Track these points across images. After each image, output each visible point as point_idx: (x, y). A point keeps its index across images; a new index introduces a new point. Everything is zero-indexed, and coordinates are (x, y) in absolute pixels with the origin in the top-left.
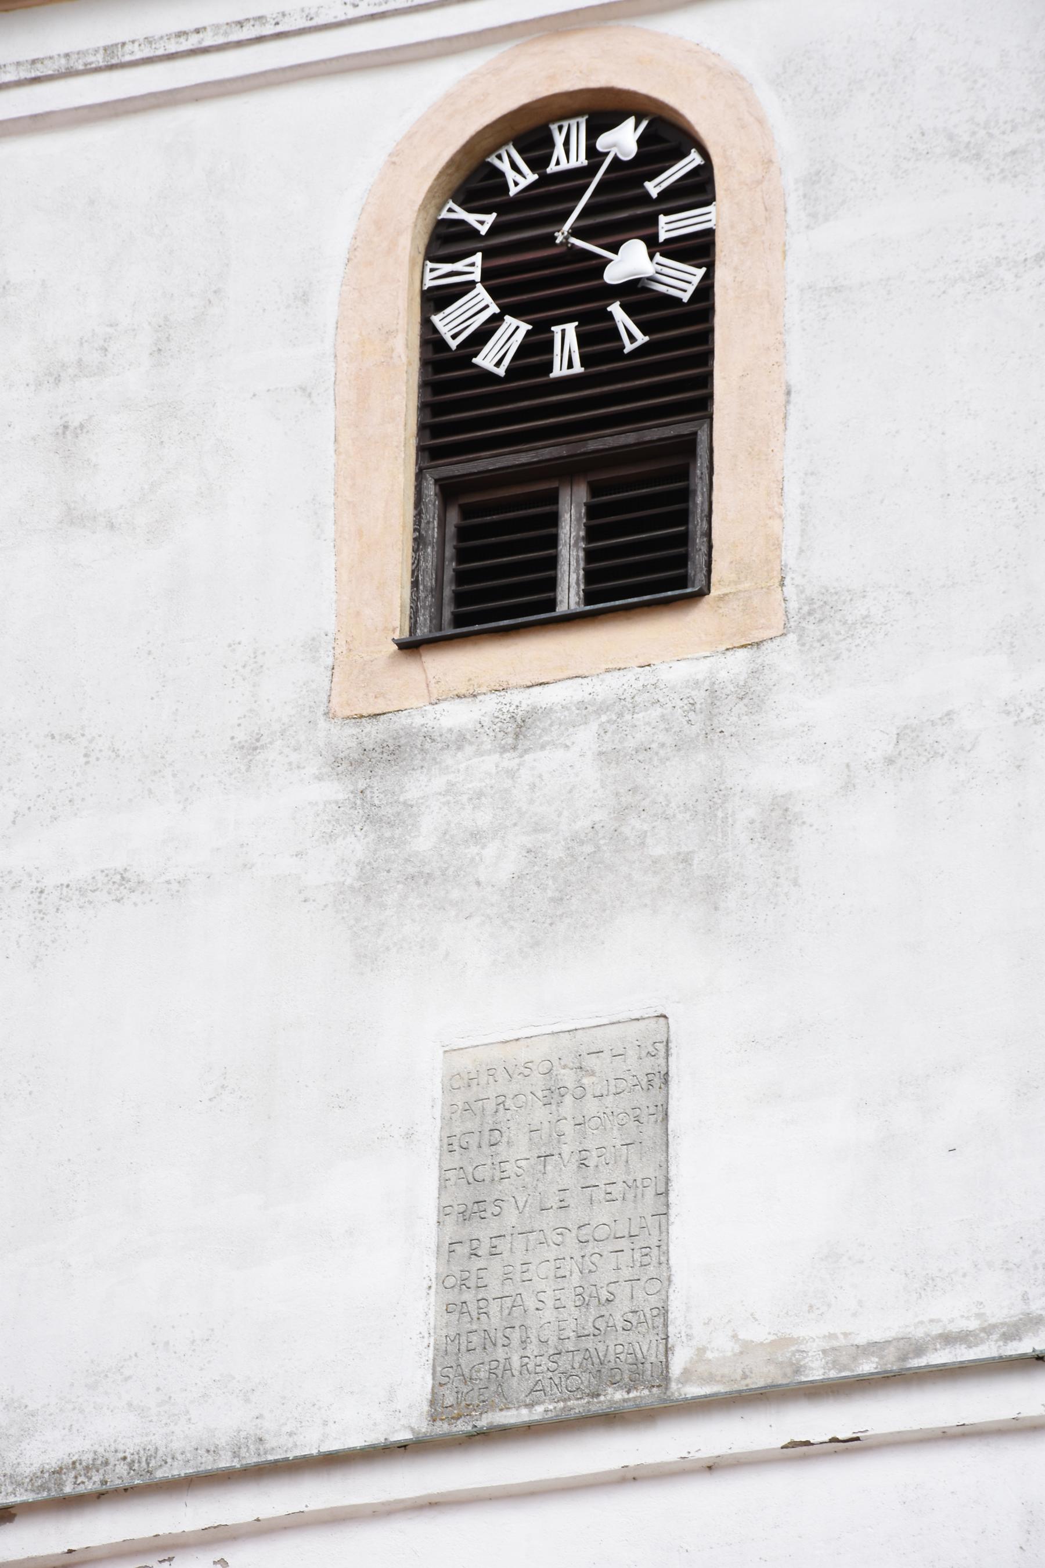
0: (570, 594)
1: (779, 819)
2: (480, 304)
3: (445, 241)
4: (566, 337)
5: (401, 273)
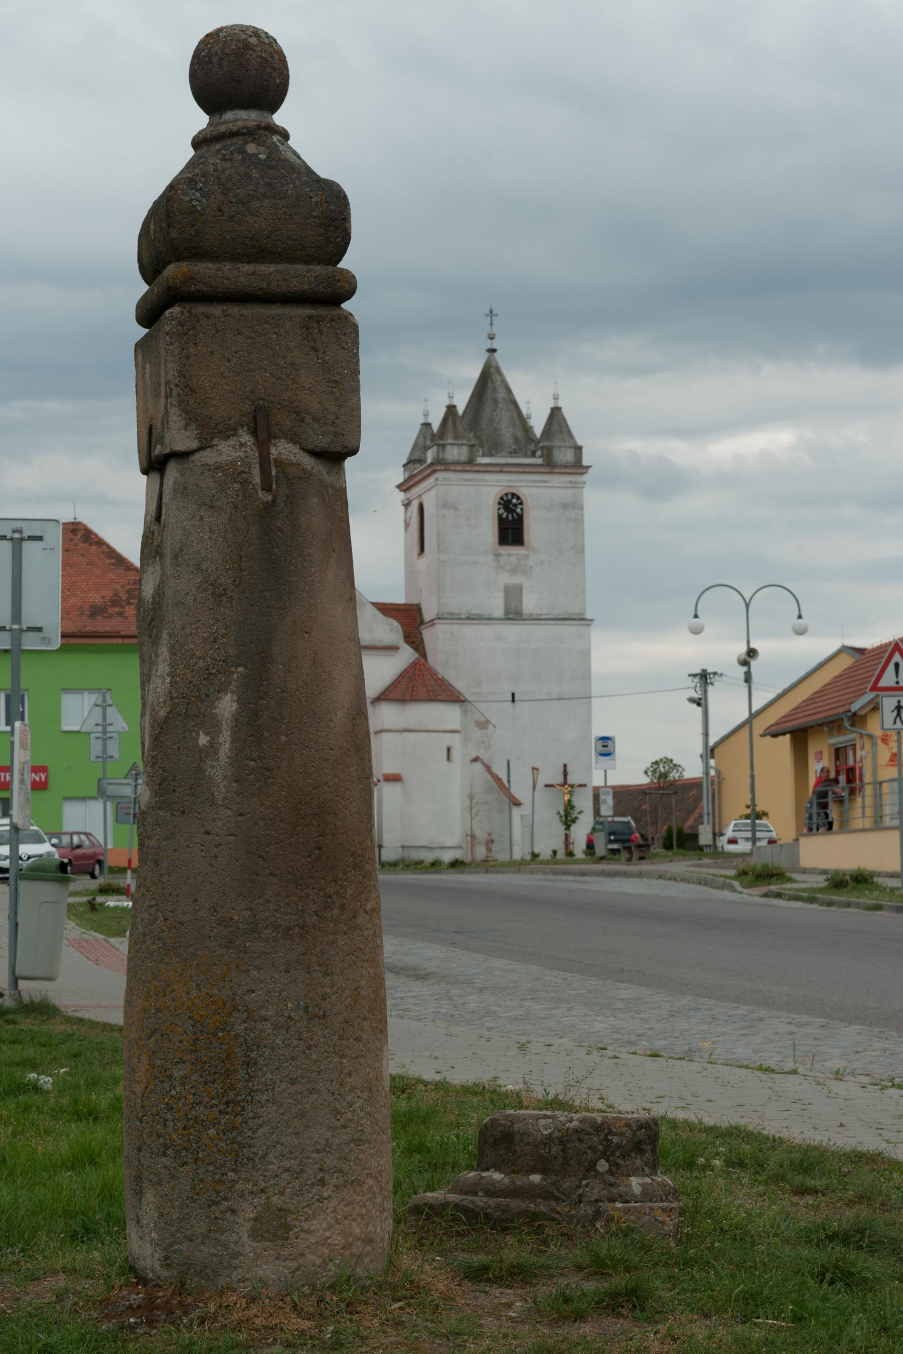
0: (510, 540)
1: (531, 568)
2: (502, 511)
3: (499, 503)
4: (510, 515)
5: (497, 506)
